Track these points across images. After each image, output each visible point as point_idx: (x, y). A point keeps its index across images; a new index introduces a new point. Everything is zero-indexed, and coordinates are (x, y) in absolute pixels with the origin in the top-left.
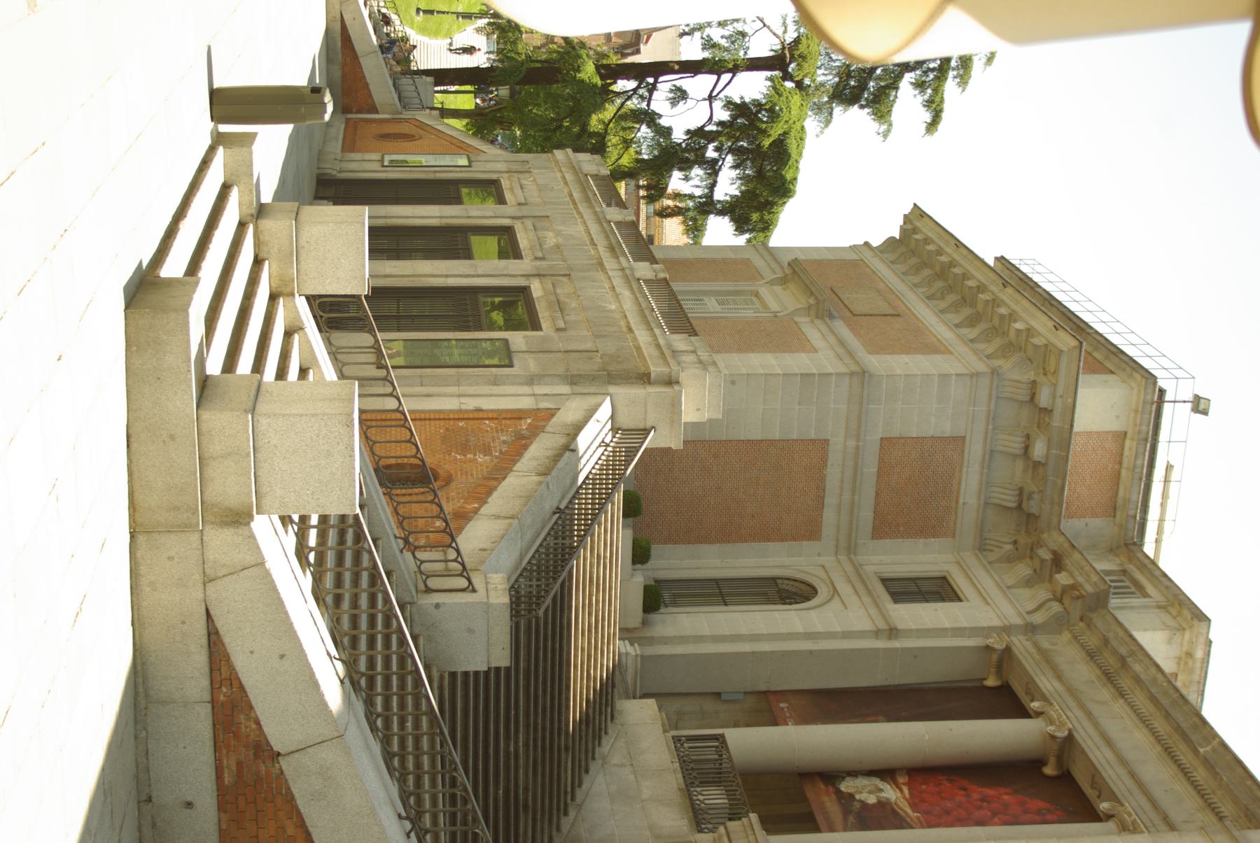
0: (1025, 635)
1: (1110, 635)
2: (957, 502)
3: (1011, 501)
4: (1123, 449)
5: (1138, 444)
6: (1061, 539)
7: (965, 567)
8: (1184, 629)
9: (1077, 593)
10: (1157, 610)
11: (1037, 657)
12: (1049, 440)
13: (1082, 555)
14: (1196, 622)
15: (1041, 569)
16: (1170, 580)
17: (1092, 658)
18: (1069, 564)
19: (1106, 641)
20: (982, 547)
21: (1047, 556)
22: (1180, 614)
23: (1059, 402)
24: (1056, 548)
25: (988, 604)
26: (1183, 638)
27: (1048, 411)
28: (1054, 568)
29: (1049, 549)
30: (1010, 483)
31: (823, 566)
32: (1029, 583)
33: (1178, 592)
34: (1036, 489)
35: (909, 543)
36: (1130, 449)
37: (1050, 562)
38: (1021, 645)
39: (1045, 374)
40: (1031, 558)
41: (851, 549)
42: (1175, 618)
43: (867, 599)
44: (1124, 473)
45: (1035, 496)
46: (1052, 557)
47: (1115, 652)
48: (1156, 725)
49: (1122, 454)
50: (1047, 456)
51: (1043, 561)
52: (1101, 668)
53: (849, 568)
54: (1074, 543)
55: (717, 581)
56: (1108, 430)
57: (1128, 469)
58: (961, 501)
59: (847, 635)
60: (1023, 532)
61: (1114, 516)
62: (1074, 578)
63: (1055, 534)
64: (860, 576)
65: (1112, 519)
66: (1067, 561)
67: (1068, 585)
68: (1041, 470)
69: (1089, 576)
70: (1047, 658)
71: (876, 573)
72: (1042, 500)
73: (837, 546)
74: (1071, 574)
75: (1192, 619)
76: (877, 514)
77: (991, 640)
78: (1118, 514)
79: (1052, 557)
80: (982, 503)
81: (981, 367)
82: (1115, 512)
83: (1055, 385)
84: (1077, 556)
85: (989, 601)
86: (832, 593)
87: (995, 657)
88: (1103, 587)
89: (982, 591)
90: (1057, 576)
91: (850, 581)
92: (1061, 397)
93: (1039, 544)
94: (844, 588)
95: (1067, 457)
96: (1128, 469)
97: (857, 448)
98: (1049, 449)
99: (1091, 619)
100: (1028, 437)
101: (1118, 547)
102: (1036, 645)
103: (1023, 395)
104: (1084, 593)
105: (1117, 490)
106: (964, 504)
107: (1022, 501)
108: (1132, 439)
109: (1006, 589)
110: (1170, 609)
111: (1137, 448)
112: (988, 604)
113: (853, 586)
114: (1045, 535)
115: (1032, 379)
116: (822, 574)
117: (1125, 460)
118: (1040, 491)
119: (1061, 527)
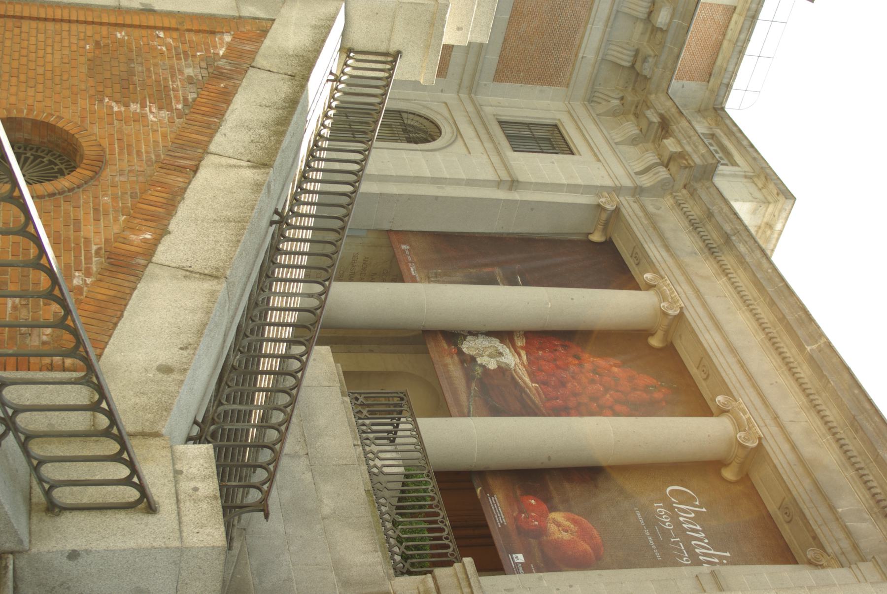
0: (633, 196)
1: (715, 209)
2: (576, 55)
3: (625, 60)
4: (729, 22)
5: (745, 20)
6: (669, 103)
7: (576, 118)
8: (769, 203)
9: (684, 162)
10: (745, 180)
11: (645, 222)
12: (674, 9)
13: (690, 123)
14: (781, 198)
15: (648, 130)
16: (756, 151)
17: (696, 228)
18: (677, 131)
19: (710, 215)
20: (591, 99)
21: (656, 119)
22: (765, 186)
24: (663, 112)
25: (599, 160)
26: (766, 210)
28: (660, 130)
29: (657, 112)
30: (627, 43)
31: (446, 103)
32: (634, 141)
33: (764, 165)
34: (652, 53)
35: (526, 88)
36: (736, 23)
37: (657, 125)
38: (630, 208)
40: (636, 116)
41: (472, 88)
42: (760, 189)
43: (489, 145)
44: (725, 44)
45: (650, 60)
46: (660, 120)
47: (719, 228)
48: (759, 311)
49: (728, 27)
50: (669, 24)
51: (651, 123)
52: (704, 241)
53: (471, 109)
54: (682, 110)
56: (720, 3)
57: (730, 40)
58: (580, 55)
59: (471, 183)
60: (630, 89)
61: (708, 82)
62: (682, 147)
63: (662, 97)
64: (481, 118)
65: (705, 83)
66: (675, 127)
67: (676, 153)
68: (659, 36)
69: (696, 147)
70: (653, 222)
71: (494, 115)
72: (656, 64)
73: (460, 85)
74: (679, 142)
75: (778, 194)
76: (502, 59)
77: (603, 200)
78: (712, 80)
79: (660, 120)
80: (599, 58)
82: (710, 78)
84: (684, 123)
85: (601, 158)
86: (455, 134)
87: (604, 216)
88: (711, 161)
89: (592, 144)
90: (665, 141)
91: (472, 123)
93: (648, 105)
94: (467, 131)
95: (689, 28)
96: (730, 40)
98: (673, 16)
99: (695, 190)
101: (706, 110)
102: (643, 208)
104: (692, 164)
105: (716, 60)
106: (583, 57)
107: (636, 61)
108: (740, 14)
109: (613, 145)
110: (756, 179)
111: (743, 23)
113: (475, 129)
114: (653, 97)
116: (446, 114)
117: (729, 33)
119: (670, 91)
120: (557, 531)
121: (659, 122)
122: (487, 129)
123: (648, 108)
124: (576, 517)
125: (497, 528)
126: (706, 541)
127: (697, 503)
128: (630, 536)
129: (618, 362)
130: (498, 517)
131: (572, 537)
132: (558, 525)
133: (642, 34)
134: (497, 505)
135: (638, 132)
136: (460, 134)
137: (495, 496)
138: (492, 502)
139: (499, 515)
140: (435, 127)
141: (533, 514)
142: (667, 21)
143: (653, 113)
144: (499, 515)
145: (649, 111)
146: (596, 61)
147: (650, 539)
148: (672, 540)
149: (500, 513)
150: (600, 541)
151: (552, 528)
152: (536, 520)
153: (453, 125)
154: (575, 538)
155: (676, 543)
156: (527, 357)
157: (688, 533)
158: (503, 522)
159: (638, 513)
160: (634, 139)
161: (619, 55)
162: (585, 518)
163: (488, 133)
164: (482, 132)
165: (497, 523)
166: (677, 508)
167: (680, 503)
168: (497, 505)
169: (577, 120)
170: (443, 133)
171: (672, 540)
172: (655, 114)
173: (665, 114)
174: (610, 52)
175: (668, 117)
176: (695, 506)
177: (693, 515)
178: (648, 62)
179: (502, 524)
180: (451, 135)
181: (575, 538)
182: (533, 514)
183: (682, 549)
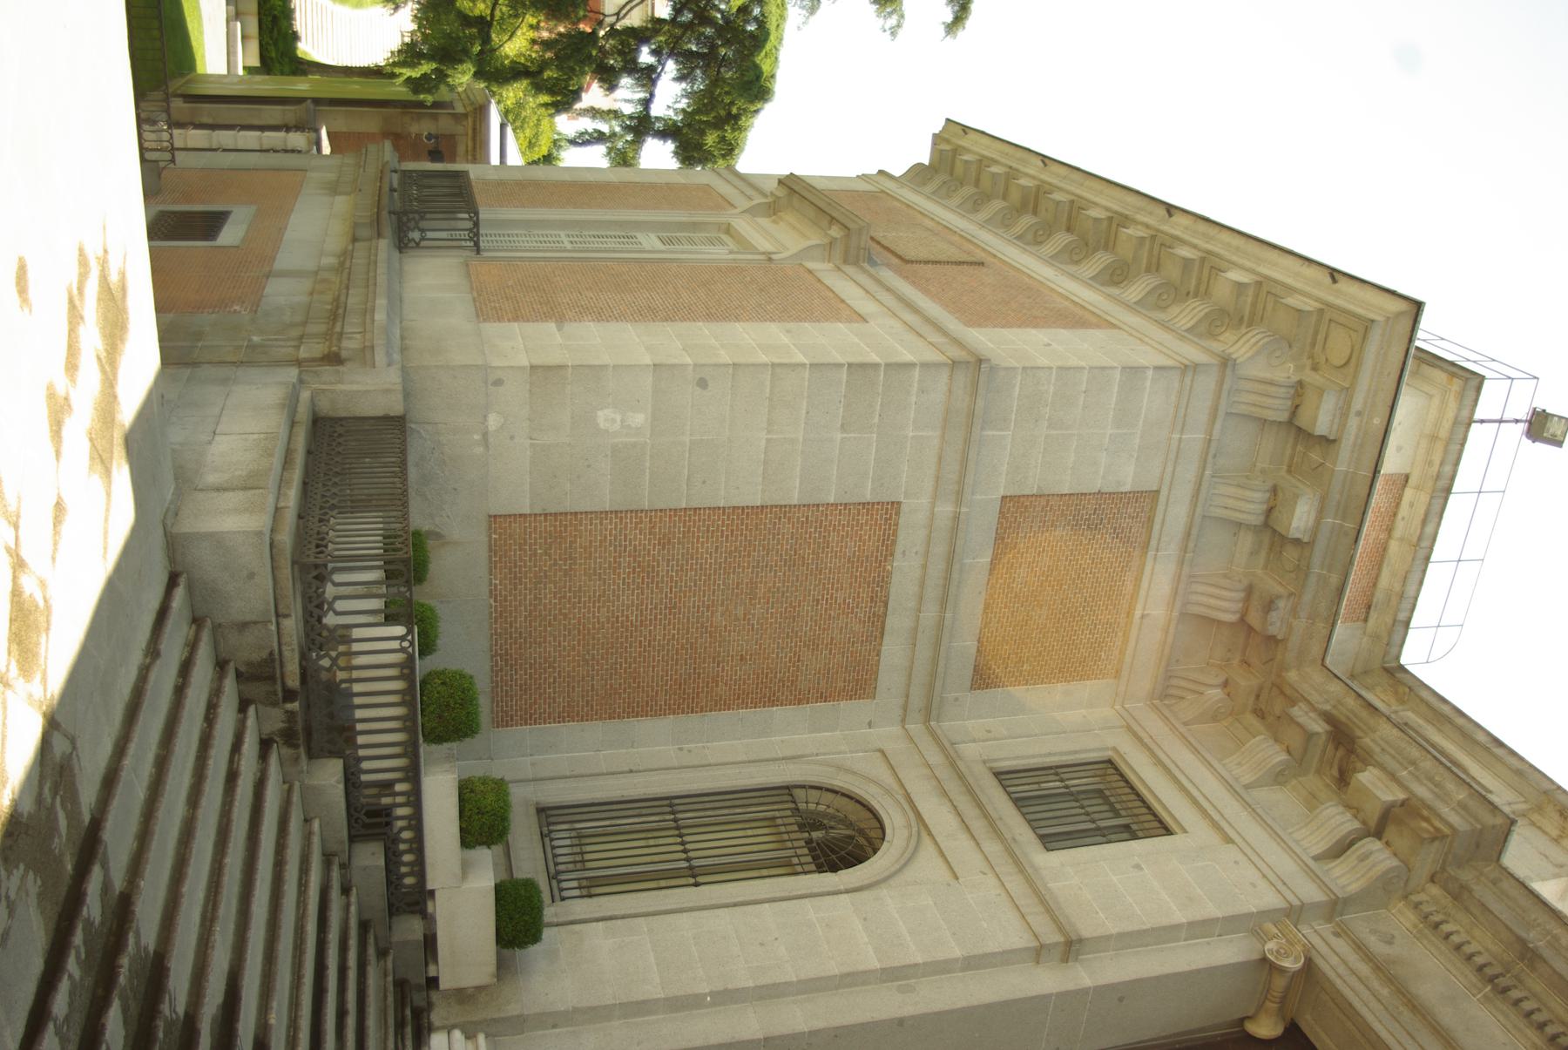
2: (1129, 614)
3: (1225, 611)
15: (1305, 750)
16: (1522, 759)
21: (1319, 727)
23: (1353, 423)
24: (1327, 707)
27: (1327, 442)
29: (1314, 709)
32: (1278, 777)
34: (1279, 589)
37: (1324, 737)
39: (1315, 368)
42: (1556, 841)
43: (992, 847)
45: (1281, 604)
46: (1328, 728)
51: (1309, 736)
55: (670, 803)
58: (1138, 613)
63: (1317, 677)
68: (1290, 554)
72: (1294, 612)
80: (1175, 614)
81: (1192, 352)
83: (1348, 392)
86: (915, 829)
89: (1201, 800)
92: (1359, 414)
97: (956, 518)
98: (1321, 512)
100: (1274, 490)
103: (1277, 410)
106: (1143, 617)
110: (1536, 817)
112: (1229, 840)
113: (955, 808)
115: (1295, 379)
118: (1291, 594)
119: (1328, 661)
121: (1327, 732)
122: (979, 805)
123: (1293, 703)
133: (1252, 553)
135: (1283, 756)
136: (926, 826)
140: (870, 815)
142: (1311, 523)
143: (1306, 713)
145: (1296, 708)
146: (1170, 621)
153: (906, 806)
160: (1281, 773)
161: (1212, 602)
163: (985, 815)
164: (970, 812)
169: (1153, 746)
170: (888, 831)
172: (1312, 715)
173: (1335, 712)
174: (1194, 598)
175: (1343, 719)
178: (1277, 608)
180: (905, 833)
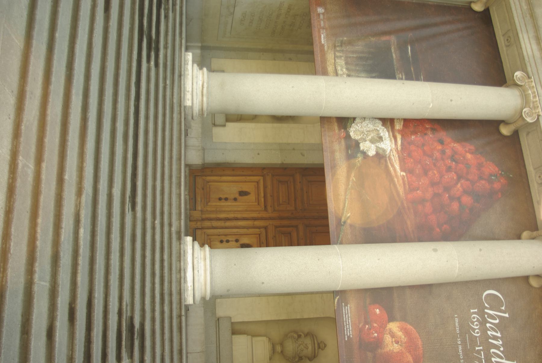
120: (390, 343)
124: (409, 327)
125: (343, 341)
126: (502, 349)
127: (503, 308)
128: (446, 345)
129: (472, 148)
130: (347, 329)
131: (401, 348)
132: (393, 335)
134: (348, 316)
137: (349, 305)
138: (345, 312)
139: (348, 327)
141: (375, 325)
144: (348, 327)
147: (460, 348)
148: (477, 348)
149: (349, 325)
150: (421, 352)
151: (388, 339)
152: (376, 332)
154: (403, 350)
155: (479, 352)
156: (402, 143)
157: (490, 340)
158: (350, 335)
159: (457, 320)
162: (415, 328)
165: (345, 335)
166: (487, 313)
167: (491, 309)
168: (348, 316)
171: (477, 348)
176: (501, 311)
177: (497, 321)
179: (349, 337)
181: (403, 350)
182: (375, 325)
183: (481, 358)
